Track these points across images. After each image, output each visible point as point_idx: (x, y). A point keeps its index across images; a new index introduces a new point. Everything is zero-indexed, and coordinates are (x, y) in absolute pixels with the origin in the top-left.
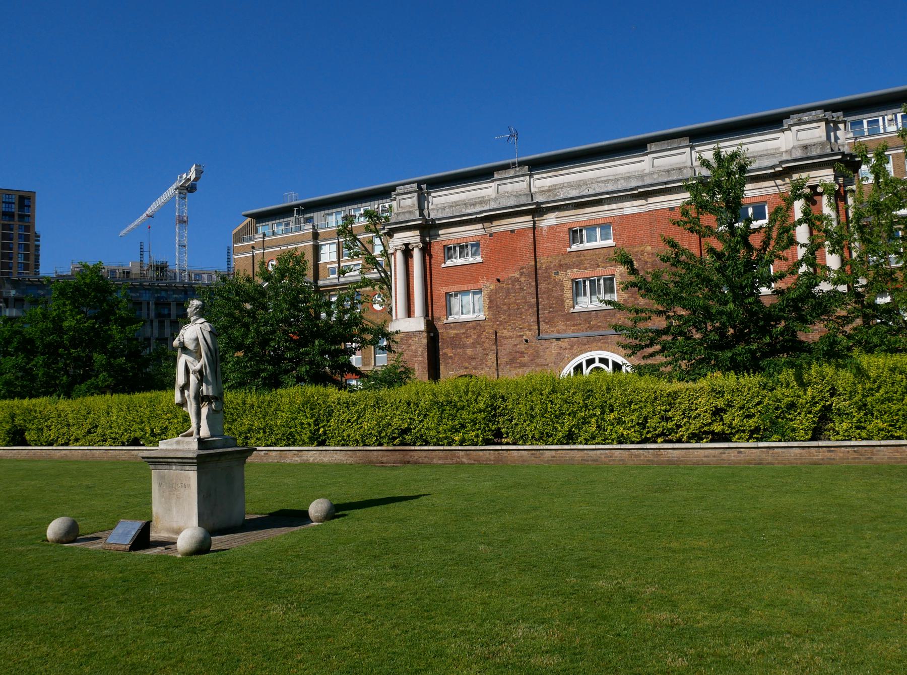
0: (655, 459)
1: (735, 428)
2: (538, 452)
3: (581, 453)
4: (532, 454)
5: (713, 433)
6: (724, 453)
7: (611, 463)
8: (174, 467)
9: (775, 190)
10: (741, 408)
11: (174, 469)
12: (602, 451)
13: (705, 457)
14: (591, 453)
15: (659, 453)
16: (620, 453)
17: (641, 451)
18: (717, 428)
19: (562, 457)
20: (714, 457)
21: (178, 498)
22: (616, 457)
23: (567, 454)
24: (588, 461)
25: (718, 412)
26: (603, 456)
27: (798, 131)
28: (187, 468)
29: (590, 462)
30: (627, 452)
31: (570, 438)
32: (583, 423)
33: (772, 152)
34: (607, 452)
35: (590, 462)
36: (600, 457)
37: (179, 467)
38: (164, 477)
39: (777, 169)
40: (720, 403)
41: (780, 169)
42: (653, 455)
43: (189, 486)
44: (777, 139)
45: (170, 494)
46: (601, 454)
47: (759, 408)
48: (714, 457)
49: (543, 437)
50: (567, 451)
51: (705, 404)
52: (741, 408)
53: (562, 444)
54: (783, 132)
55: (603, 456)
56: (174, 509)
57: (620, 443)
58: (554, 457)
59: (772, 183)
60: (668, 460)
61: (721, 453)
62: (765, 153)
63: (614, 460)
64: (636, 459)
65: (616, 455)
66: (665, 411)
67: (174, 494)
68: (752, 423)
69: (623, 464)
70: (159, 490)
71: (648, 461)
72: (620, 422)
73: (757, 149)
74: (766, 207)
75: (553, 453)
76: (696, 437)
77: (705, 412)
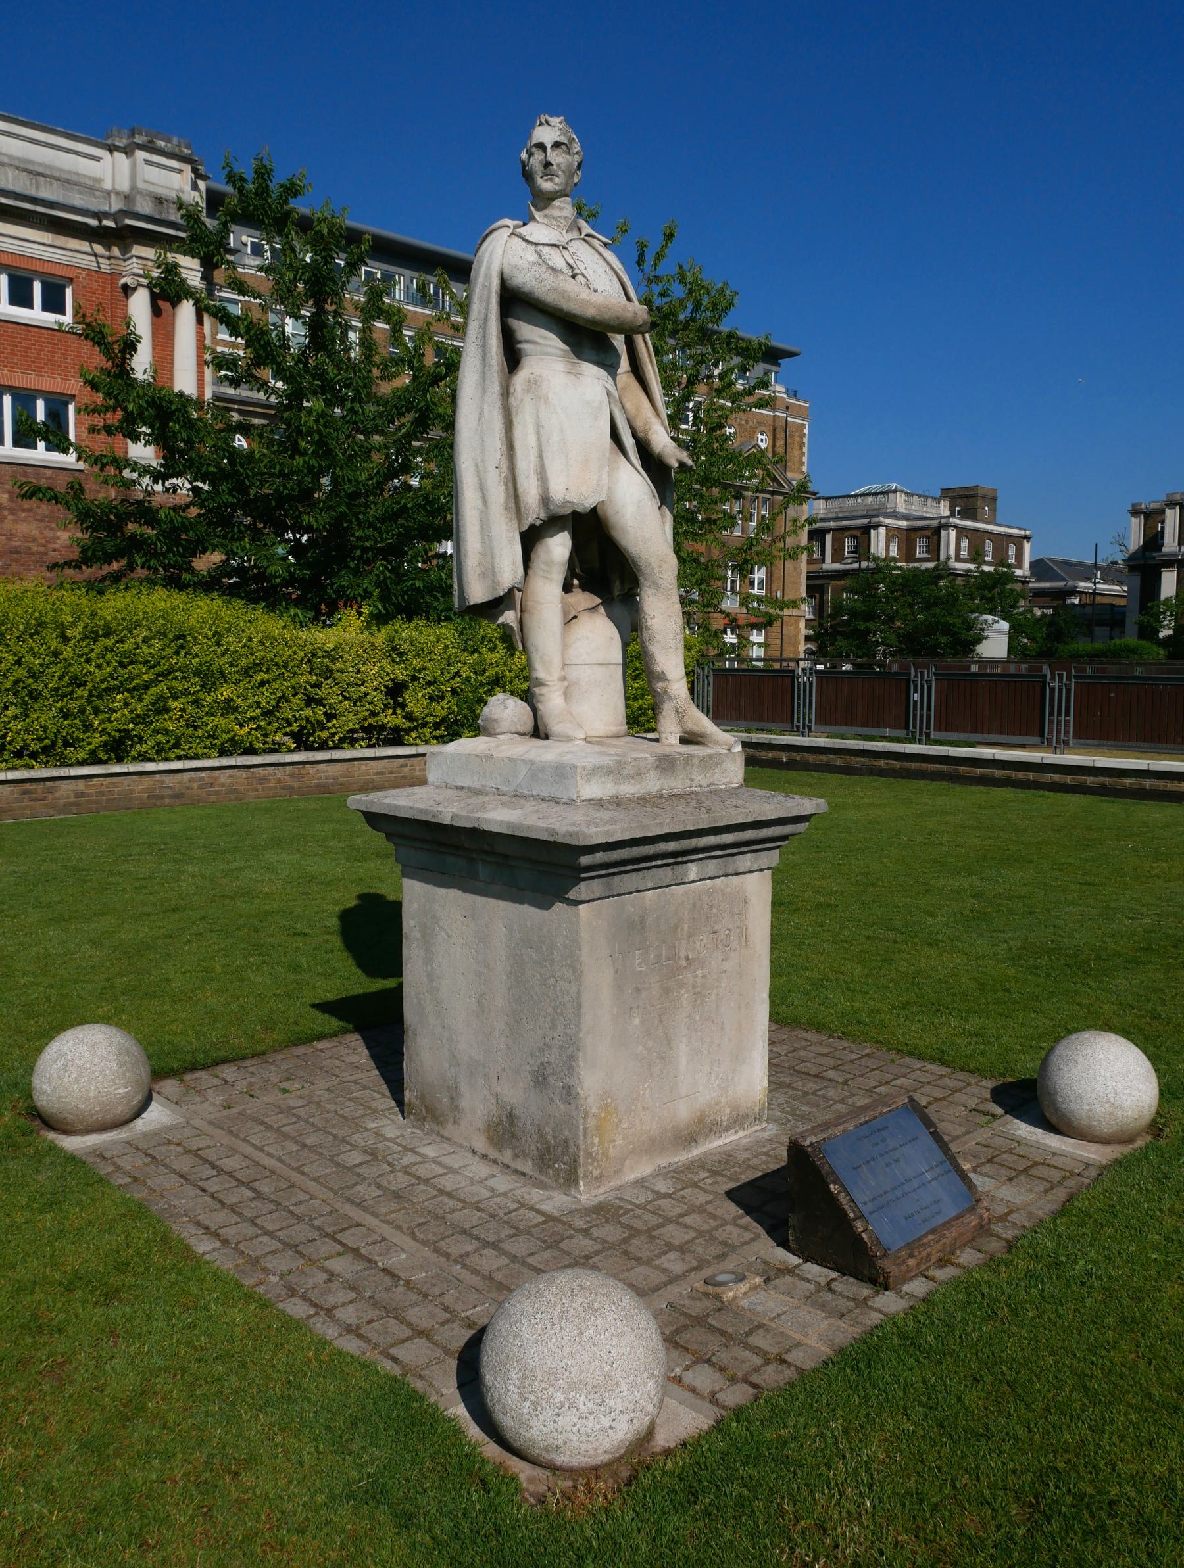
0: (296, 785)
1: (416, 720)
2: (40, 787)
3: (146, 782)
4: (25, 792)
5: (382, 727)
6: (406, 766)
7: (213, 798)
8: (693, 870)
9: (89, 262)
10: (429, 684)
11: (692, 876)
12: (193, 774)
13: (378, 774)
14: (168, 779)
15: (303, 772)
16: (230, 777)
17: (271, 770)
18: (391, 719)
19: (103, 794)
20: (391, 773)
21: (699, 996)
22: (223, 785)
23: (115, 785)
24: (162, 797)
25: (395, 690)
26: (195, 785)
27: (147, 162)
28: (745, 861)
29: (167, 801)
30: (244, 774)
31: (117, 749)
32: (159, 712)
33: (88, 182)
34: (203, 774)
35: (167, 801)
36: (188, 788)
37: (712, 867)
38: (642, 922)
39: (106, 223)
40: (402, 674)
41: (112, 224)
42: (292, 775)
43: (743, 935)
44: (97, 159)
45: (667, 991)
46: (191, 780)
47: (456, 683)
48: (391, 773)
49: (48, 752)
50: (115, 779)
51: (378, 671)
52: (429, 684)
53: (99, 762)
54: (111, 151)
55: (195, 785)
56: (684, 1047)
57: (223, 753)
58: (82, 795)
59: (85, 246)
60: (318, 785)
61: (402, 766)
62: (75, 178)
63: (218, 792)
64: (260, 787)
65: (222, 780)
66: (314, 686)
67: (681, 985)
68: (440, 710)
69: (236, 799)
70: (619, 988)
71: (283, 788)
72: (229, 707)
73: (58, 164)
74: (69, 292)
75: (81, 785)
76: (349, 740)
77: (376, 689)
